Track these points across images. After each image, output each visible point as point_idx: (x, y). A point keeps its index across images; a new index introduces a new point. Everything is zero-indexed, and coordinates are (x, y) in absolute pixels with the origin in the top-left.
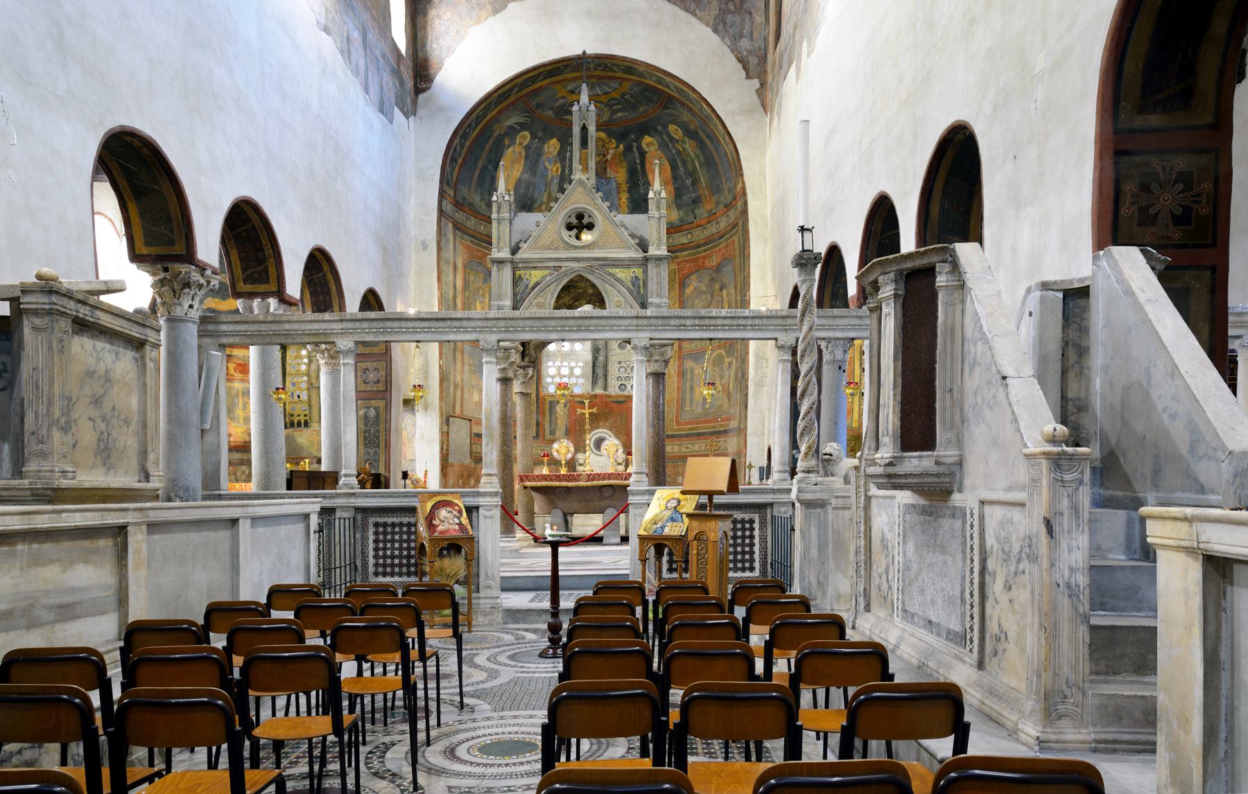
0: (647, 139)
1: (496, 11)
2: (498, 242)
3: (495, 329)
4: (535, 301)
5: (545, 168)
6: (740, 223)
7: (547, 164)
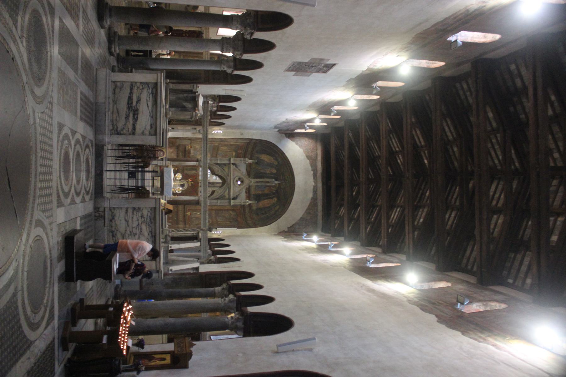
0: (275, 199)
1: (307, 157)
2: (235, 160)
5: (268, 169)
7: (269, 169)
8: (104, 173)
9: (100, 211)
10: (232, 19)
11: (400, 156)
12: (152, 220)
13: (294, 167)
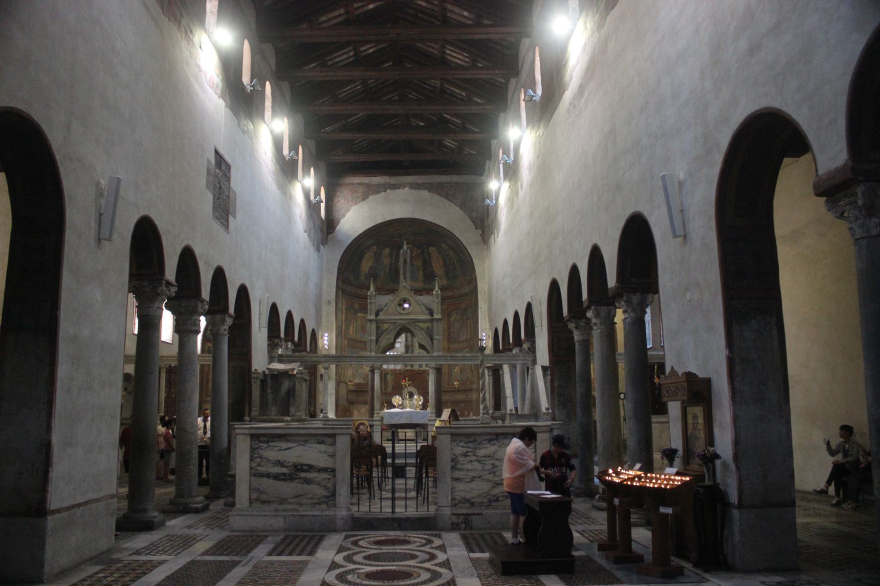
0: (431, 249)
1: (364, 199)
4: (386, 337)
5: (383, 261)
8: (396, 516)
9: (458, 522)
10: (145, 316)
11: (362, 49)
12: (472, 439)
13: (380, 220)
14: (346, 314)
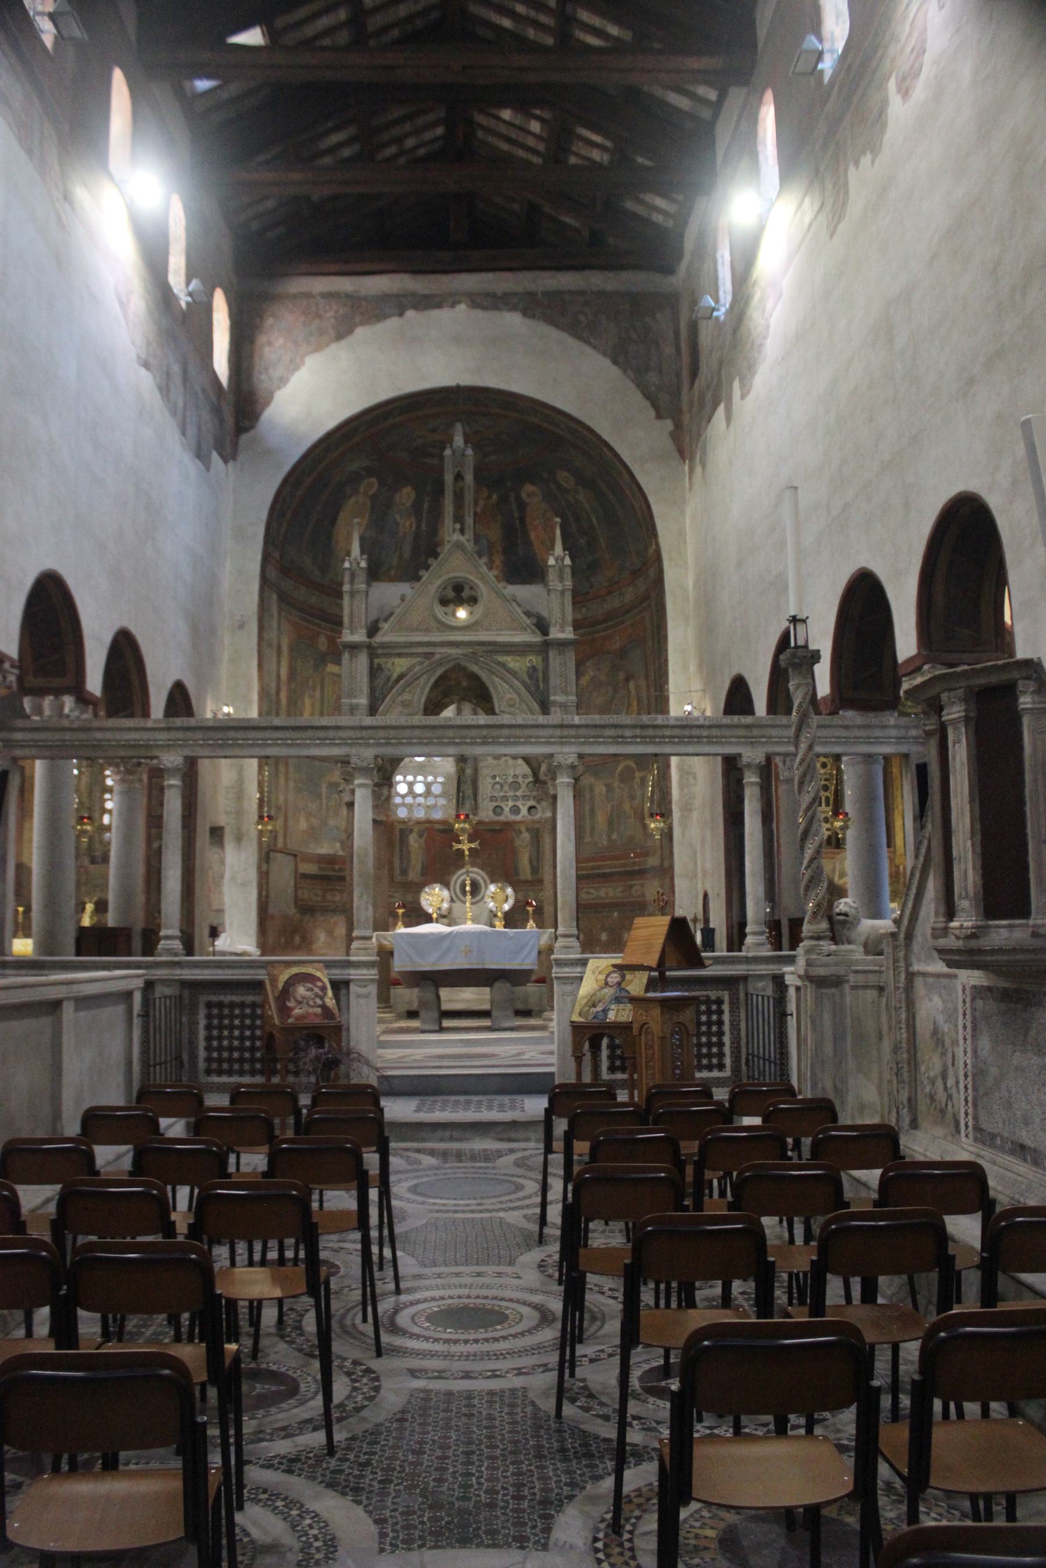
0: (529, 488)
1: (340, 337)
2: (351, 622)
3: (371, 741)
4: (400, 699)
5: (398, 524)
6: (653, 595)
7: (398, 517)
13: (385, 392)
14: (292, 659)
